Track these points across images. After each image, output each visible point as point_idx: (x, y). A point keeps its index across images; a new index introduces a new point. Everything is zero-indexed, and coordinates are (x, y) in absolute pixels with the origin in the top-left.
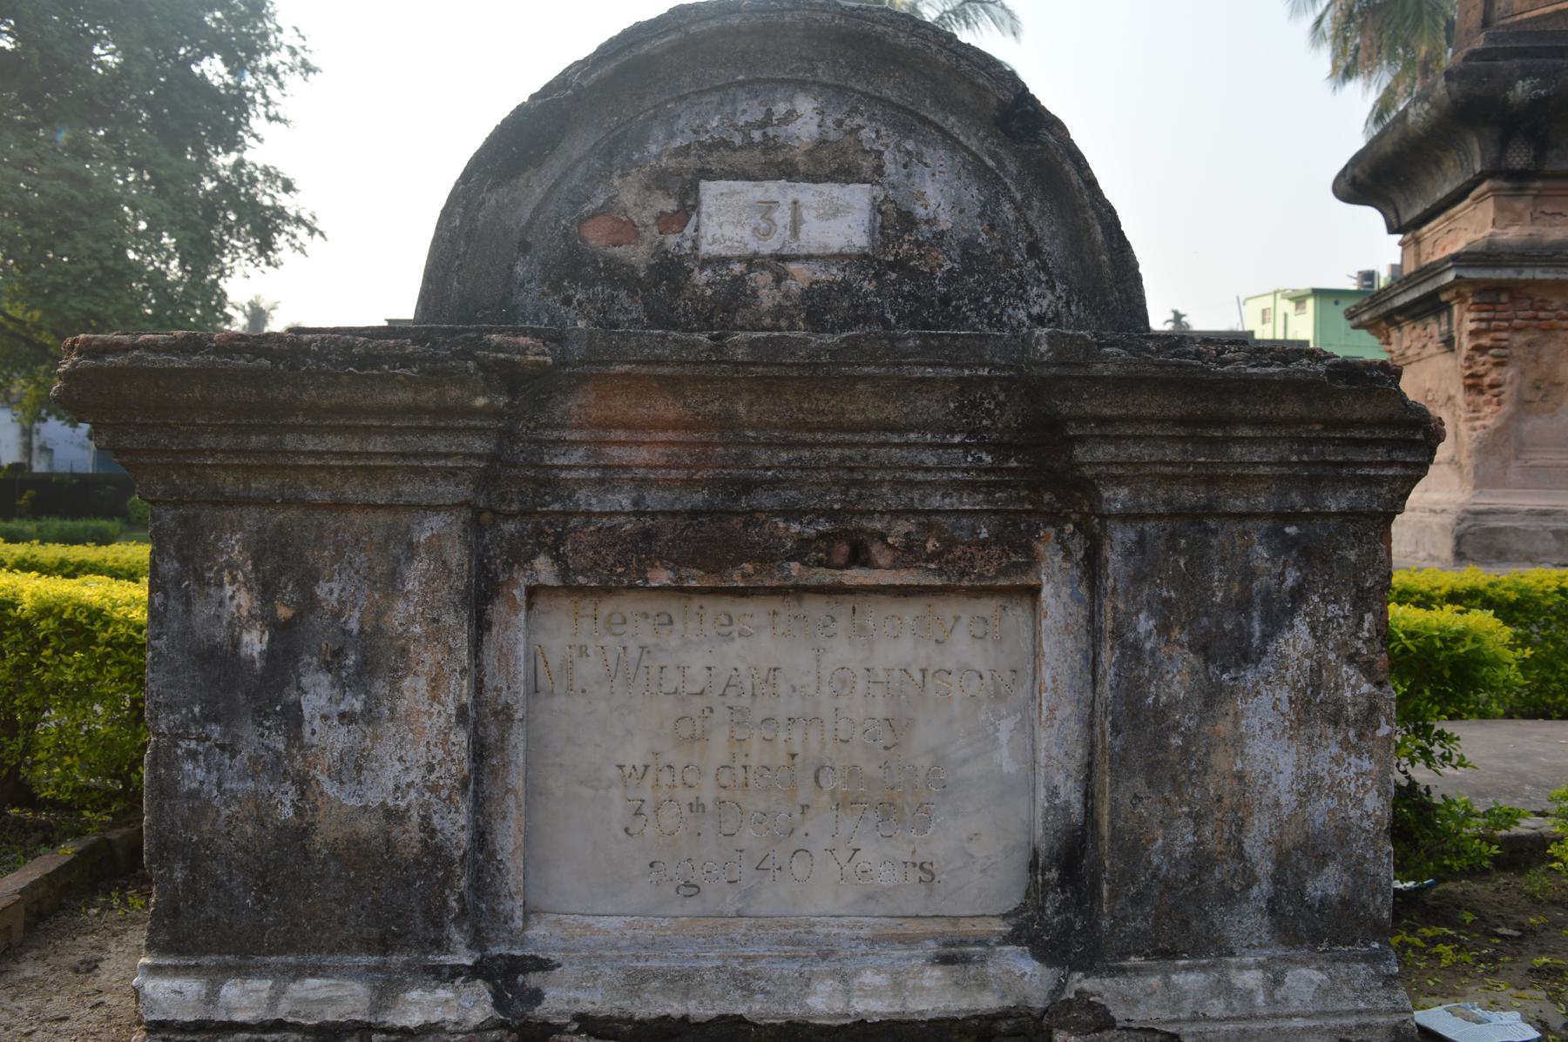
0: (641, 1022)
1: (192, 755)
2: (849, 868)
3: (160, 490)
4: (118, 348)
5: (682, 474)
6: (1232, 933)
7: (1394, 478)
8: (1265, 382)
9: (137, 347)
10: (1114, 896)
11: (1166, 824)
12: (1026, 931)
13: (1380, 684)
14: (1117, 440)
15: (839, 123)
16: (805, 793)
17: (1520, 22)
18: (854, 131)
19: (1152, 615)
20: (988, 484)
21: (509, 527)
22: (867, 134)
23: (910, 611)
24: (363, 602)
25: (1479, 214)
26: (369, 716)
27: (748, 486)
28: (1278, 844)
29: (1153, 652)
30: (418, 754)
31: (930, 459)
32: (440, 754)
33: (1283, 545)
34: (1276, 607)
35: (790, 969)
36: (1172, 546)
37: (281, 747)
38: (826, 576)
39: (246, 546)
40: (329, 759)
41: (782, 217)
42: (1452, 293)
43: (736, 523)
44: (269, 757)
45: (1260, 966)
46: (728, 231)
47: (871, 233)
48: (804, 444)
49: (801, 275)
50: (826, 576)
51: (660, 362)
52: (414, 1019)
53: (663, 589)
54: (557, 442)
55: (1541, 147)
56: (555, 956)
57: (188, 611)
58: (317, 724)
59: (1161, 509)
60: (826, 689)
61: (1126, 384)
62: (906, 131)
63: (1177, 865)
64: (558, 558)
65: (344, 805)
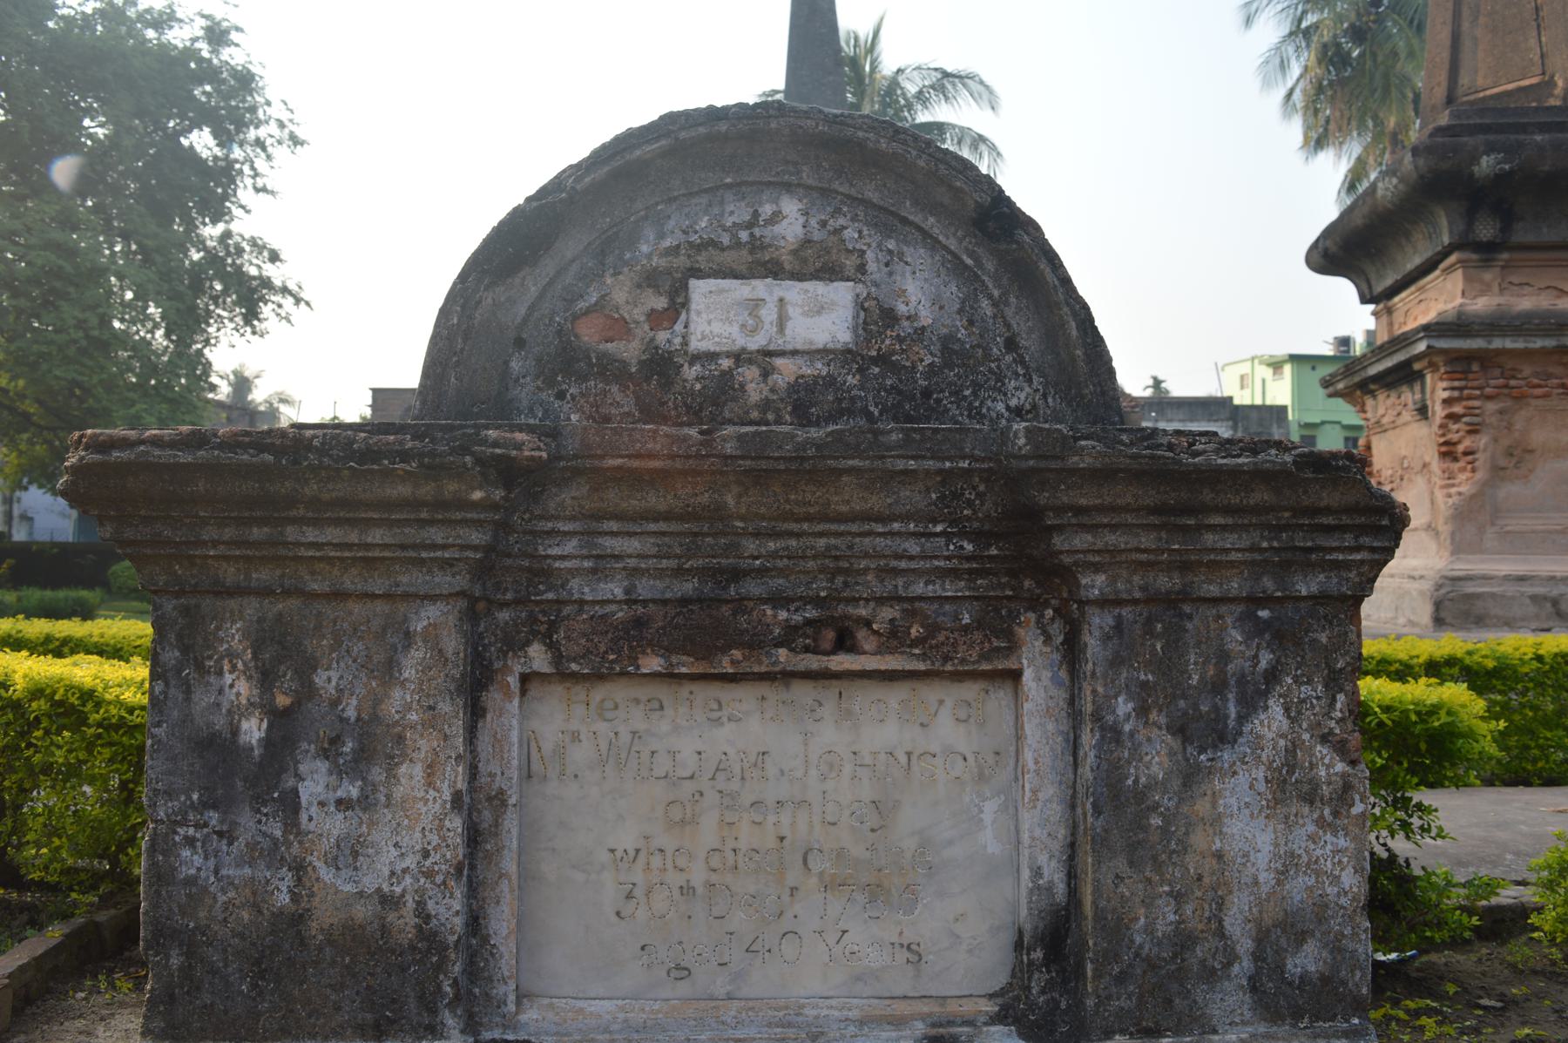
1: (190, 842)
2: (837, 950)
3: (162, 580)
4: (125, 444)
5: (673, 563)
6: (1215, 1011)
7: (1362, 562)
8: (1235, 472)
9: (143, 442)
10: (1098, 976)
11: (1148, 903)
13: (1353, 763)
14: (1092, 528)
15: (823, 224)
16: (793, 876)
17: (1484, 98)
18: (838, 231)
19: (1130, 698)
20: (970, 572)
21: (504, 616)
22: (850, 234)
23: (895, 695)
24: (360, 690)
25: (1449, 285)
27: (736, 575)
28: (1258, 922)
29: (1132, 734)
30: (414, 840)
31: (913, 547)
32: (435, 840)
33: (1257, 630)
36: (1149, 630)
37: (278, 833)
38: (813, 662)
39: (246, 635)
40: (325, 845)
41: (769, 314)
42: (1424, 363)
43: (726, 610)
44: (266, 844)
46: (717, 328)
47: (855, 329)
48: (791, 534)
49: (787, 370)
50: (813, 662)
51: (651, 456)
53: (655, 675)
54: (551, 533)
55: (1508, 219)
57: (188, 699)
58: (314, 810)
59: (1137, 595)
60: (813, 772)
61: (1102, 475)
62: (887, 231)
63: (1159, 944)
64: (552, 646)
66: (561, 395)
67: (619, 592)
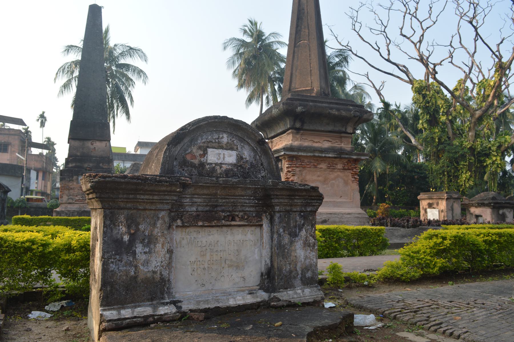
1: (112, 262)
3: (107, 206)
4: (109, 177)
5: (206, 204)
8: (301, 189)
9: (113, 177)
10: (278, 279)
11: (285, 265)
15: (231, 139)
17: (297, 91)
18: (233, 141)
22: (235, 142)
23: (240, 229)
24: (149, 229)
25: (288, 138)
26: (150, 252)
27: (216, 206)
30: (159, 259)
31: (247, 201)
32: (164, 259)
33: (301, 216)
35: (225, 298)
37: (132, 260)
38: (228, 223)
39: (124, 218)
40: (141, 261)
41: (222, 156)
42: (283, 157)
43: (213, 213)
44: (129, 262)
46: (212, 158)
48: (228, 199)
49: (224, 167)
50: (228, 223)
51: (208, 183)
52: (162, 313)
53: (201, 226)
55: (303, 122)
56: (182, 300)
57: (112, 232)
58: (139, 254)
62: (242, 142)
64: (182, 220)
65: (144, 271)
66: (183, 170)
67: (195, 209)
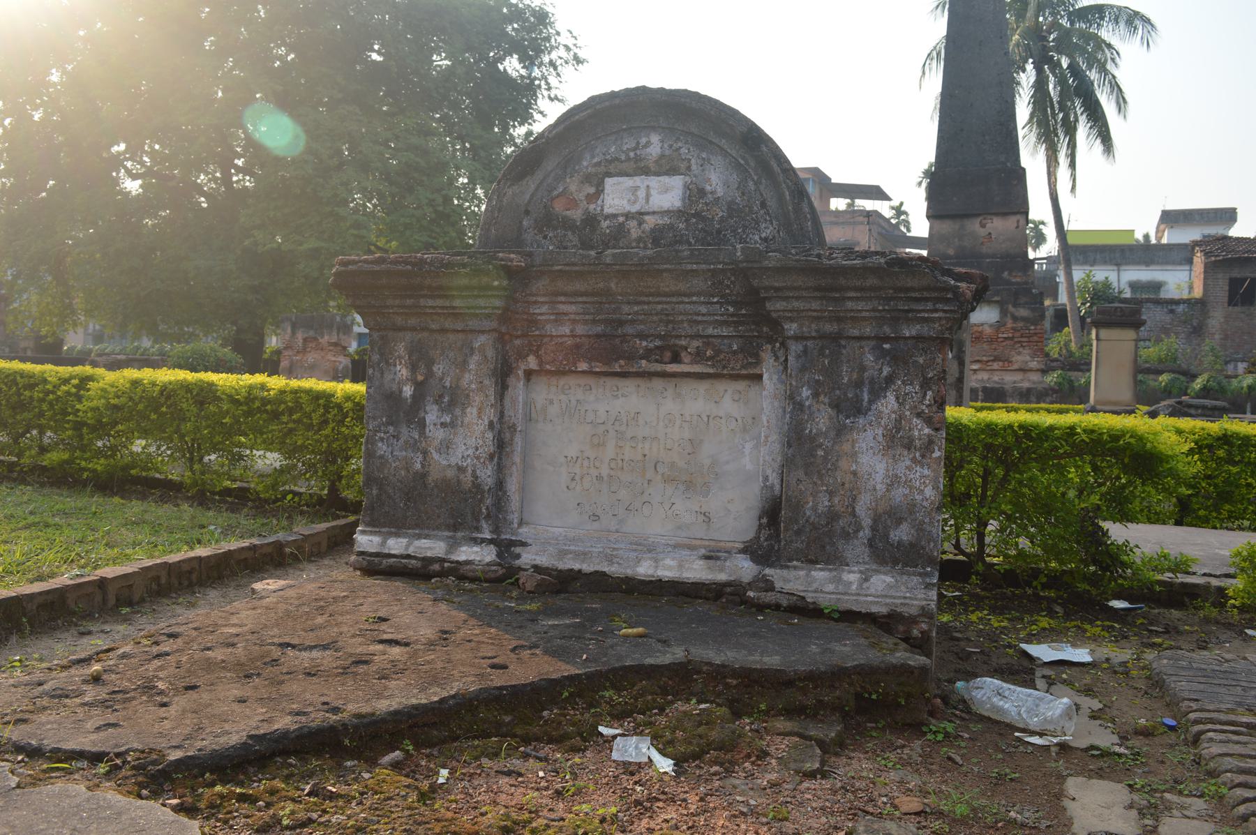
0: (561, 571)
1: (382, 439)
2: (670, 512)
5: (591, 317)
6: (848, 555)
7: (940, 318)
8: (853, 269)
10: (786, 530)
12: (750, 550)
13: (937, 430)
14: (786, 299)
15: (671, 146)
16: (650, 474)
19: (809, 388)
20: (734, 322)
21: (518, 342)
23: (702, 387)
26: (452, 425)
27: (621, 323)
28: (875, 510)
29: (809, 407)
30: (472, 442)
31: (703, 309)
32: (481, 442)
33: (882, 354)
34: (877, 386)
35: (633, 555)
36: (821, 353)
38: (658, 367)
39: (406, 348)
40: (436, 443)
41: (641, 194)
43: (617, 341)
44: (412, 441)
45: (861, 572)
46: (616, 202)
47: (683, 200)
48: (644, 303)
49: (651, 221)
50: (658, 367)
51: (574, 264)
52: (462, 558)
53: (583, 372)
54: (535, 302)
56: (529, 541)
59: (814, 334)
60: (661, 424)
61: (783, 270)
63: (820, 516)
64: (538, 357)
65: (442, 464)
66: (545, 237)
67: (568, 331)
